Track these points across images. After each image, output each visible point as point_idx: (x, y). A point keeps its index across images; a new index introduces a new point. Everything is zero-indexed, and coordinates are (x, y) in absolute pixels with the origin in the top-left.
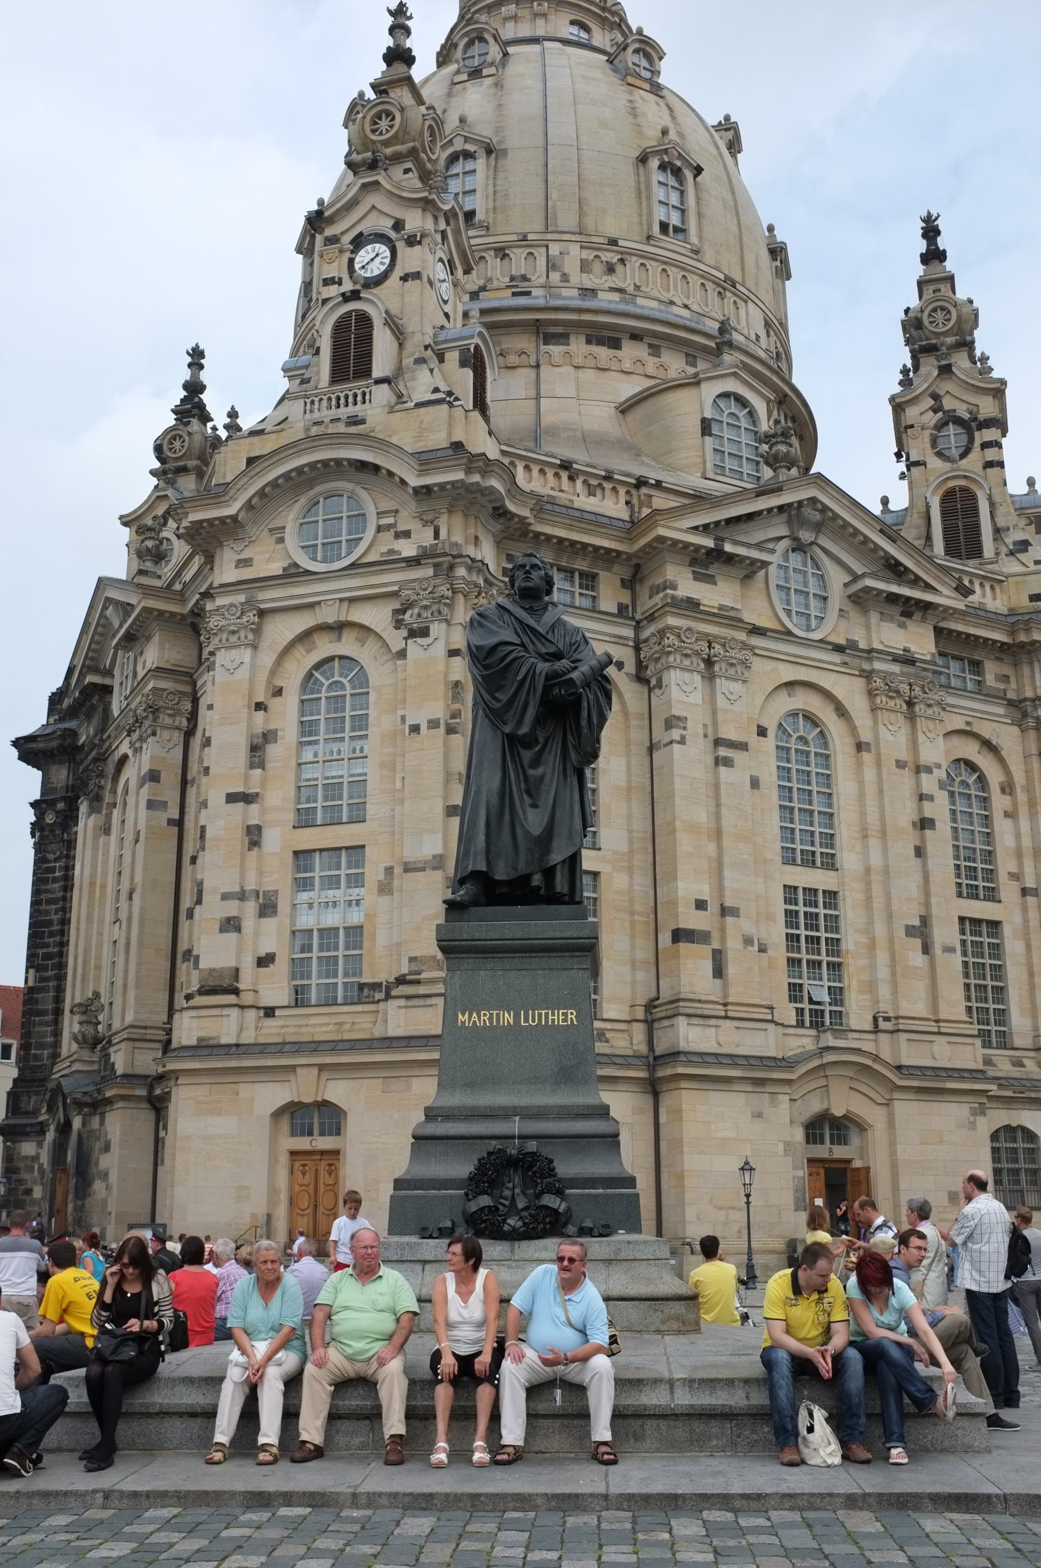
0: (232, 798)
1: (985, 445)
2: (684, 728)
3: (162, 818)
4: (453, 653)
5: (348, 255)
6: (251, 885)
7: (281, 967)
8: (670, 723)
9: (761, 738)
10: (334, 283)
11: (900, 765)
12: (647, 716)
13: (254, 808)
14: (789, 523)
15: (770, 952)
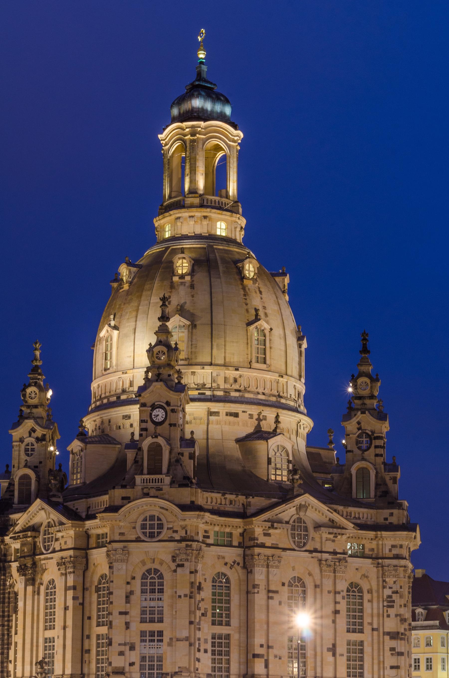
0: (121, 613)
1: (376, 447)
2: (259, 588)
3: (78, 602)
4: (191, 572)
5: (149, 411)
6: (128, 641)
7: (137, 667)
8: (254, 586)
9: (283, 587)
10: (145, 422)
11: (329, 592)
12: (246, 581)
13: (128, 616)
14: (296, 509)
15: (282, 659)
